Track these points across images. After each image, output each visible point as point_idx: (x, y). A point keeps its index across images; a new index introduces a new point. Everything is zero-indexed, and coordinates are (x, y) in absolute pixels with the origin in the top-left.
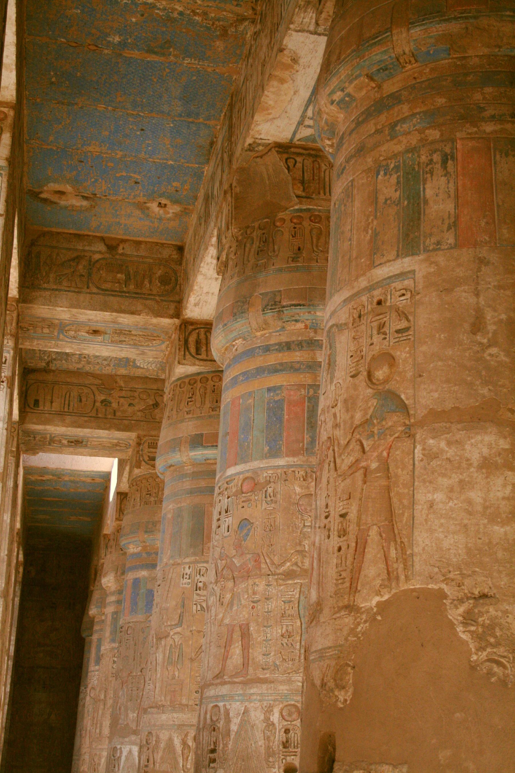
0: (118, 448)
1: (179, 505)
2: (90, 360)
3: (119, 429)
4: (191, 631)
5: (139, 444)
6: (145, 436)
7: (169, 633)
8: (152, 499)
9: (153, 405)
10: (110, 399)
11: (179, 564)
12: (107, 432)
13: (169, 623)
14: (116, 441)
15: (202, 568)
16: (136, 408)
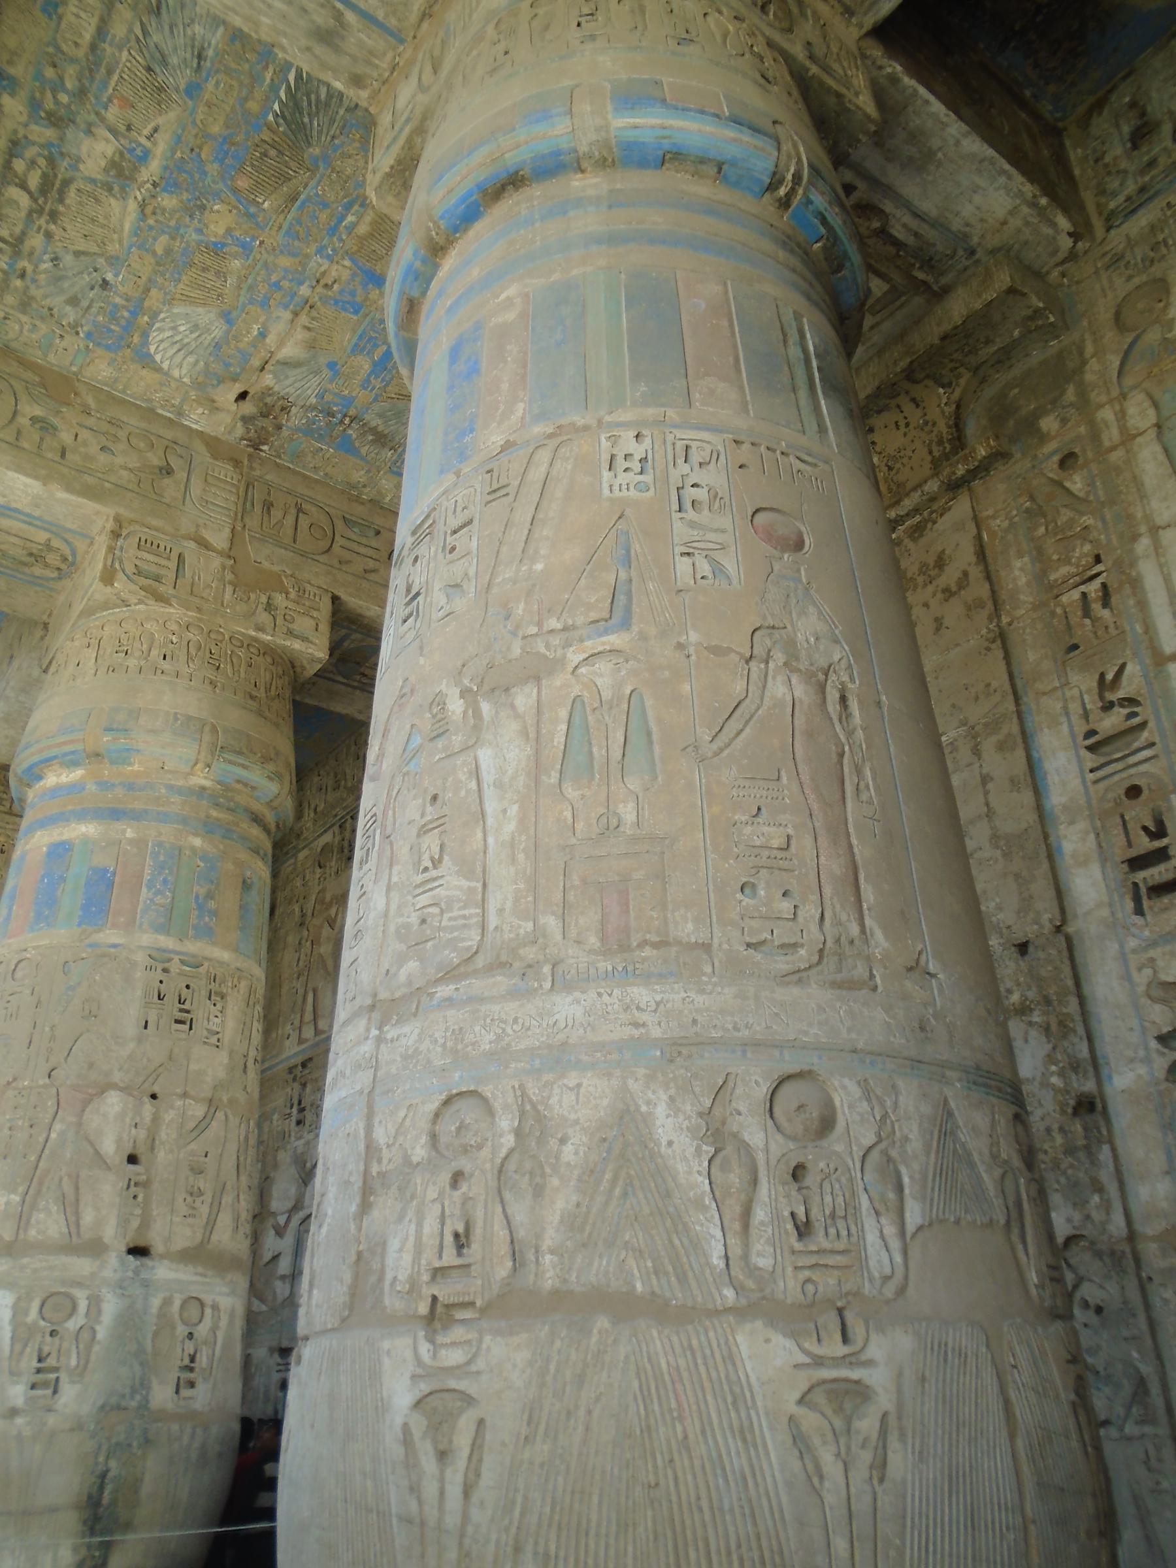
0: (38, 570)
1: (556, 277)
2: (33, 291)
3: (69, 489)
4: (680, 646)
5: (116, 535)
6: (131, 521)
7: (562, 661)
8: (132, 662)
9: (161, 469)
10: (55, 421)
11: (586, 428)
12: (34, 486)
13: (554, 623)
14: (42, 536)
15: (694, 445)
16: (119, 460)
